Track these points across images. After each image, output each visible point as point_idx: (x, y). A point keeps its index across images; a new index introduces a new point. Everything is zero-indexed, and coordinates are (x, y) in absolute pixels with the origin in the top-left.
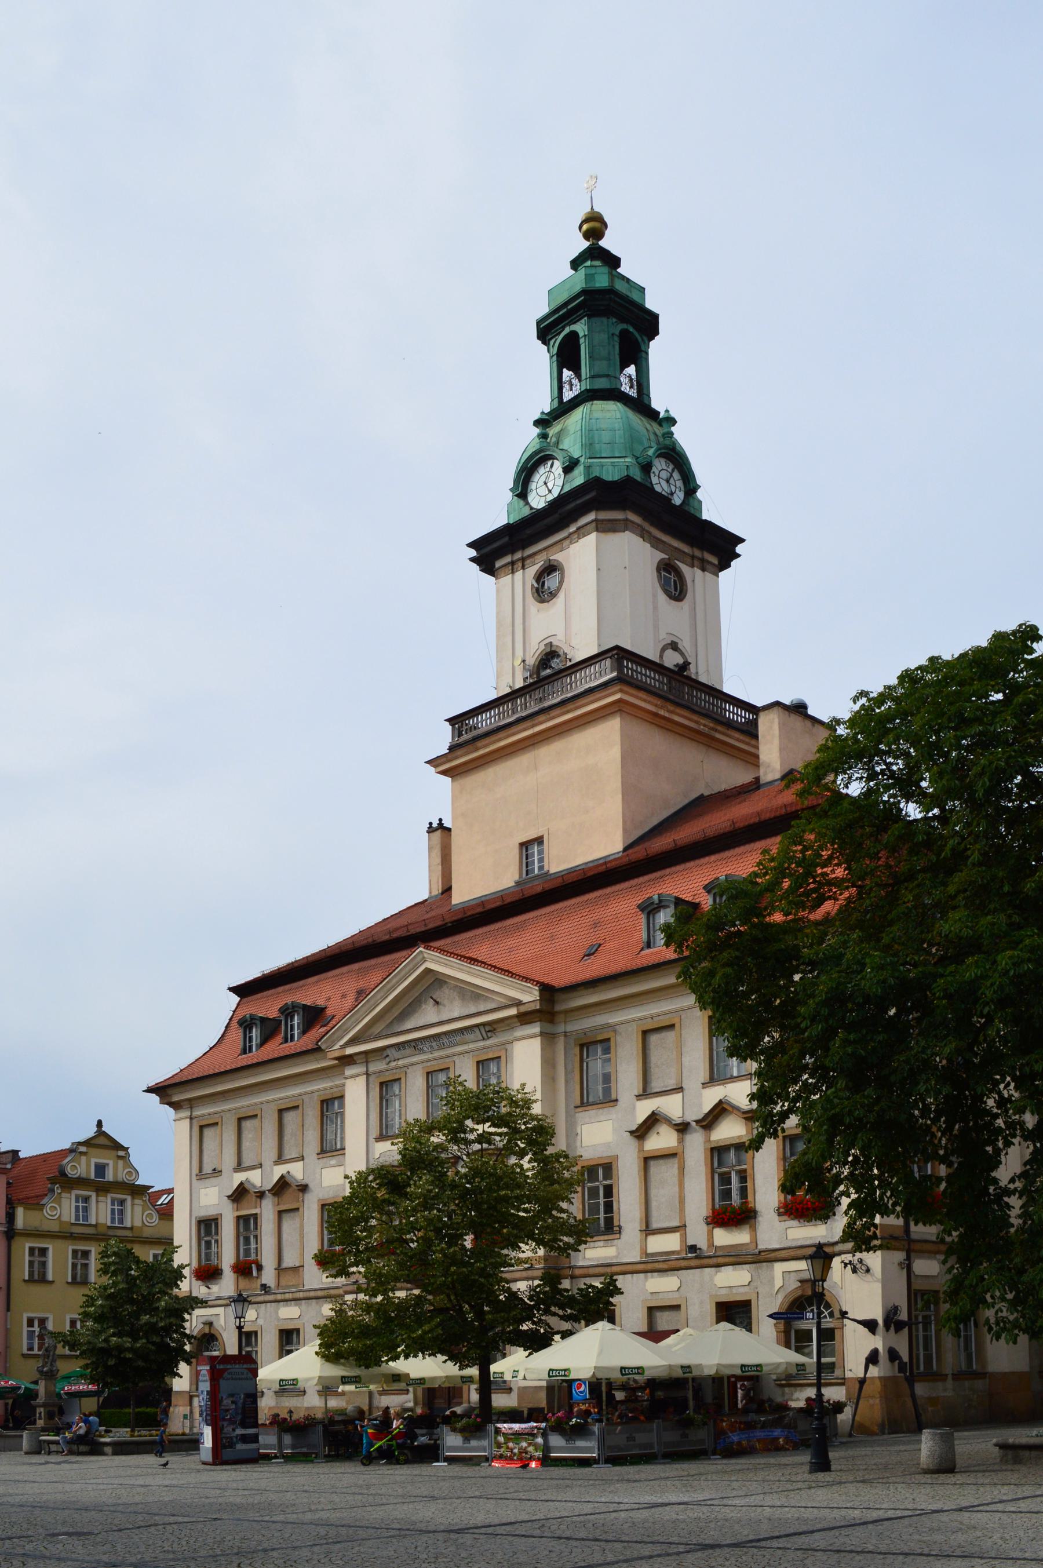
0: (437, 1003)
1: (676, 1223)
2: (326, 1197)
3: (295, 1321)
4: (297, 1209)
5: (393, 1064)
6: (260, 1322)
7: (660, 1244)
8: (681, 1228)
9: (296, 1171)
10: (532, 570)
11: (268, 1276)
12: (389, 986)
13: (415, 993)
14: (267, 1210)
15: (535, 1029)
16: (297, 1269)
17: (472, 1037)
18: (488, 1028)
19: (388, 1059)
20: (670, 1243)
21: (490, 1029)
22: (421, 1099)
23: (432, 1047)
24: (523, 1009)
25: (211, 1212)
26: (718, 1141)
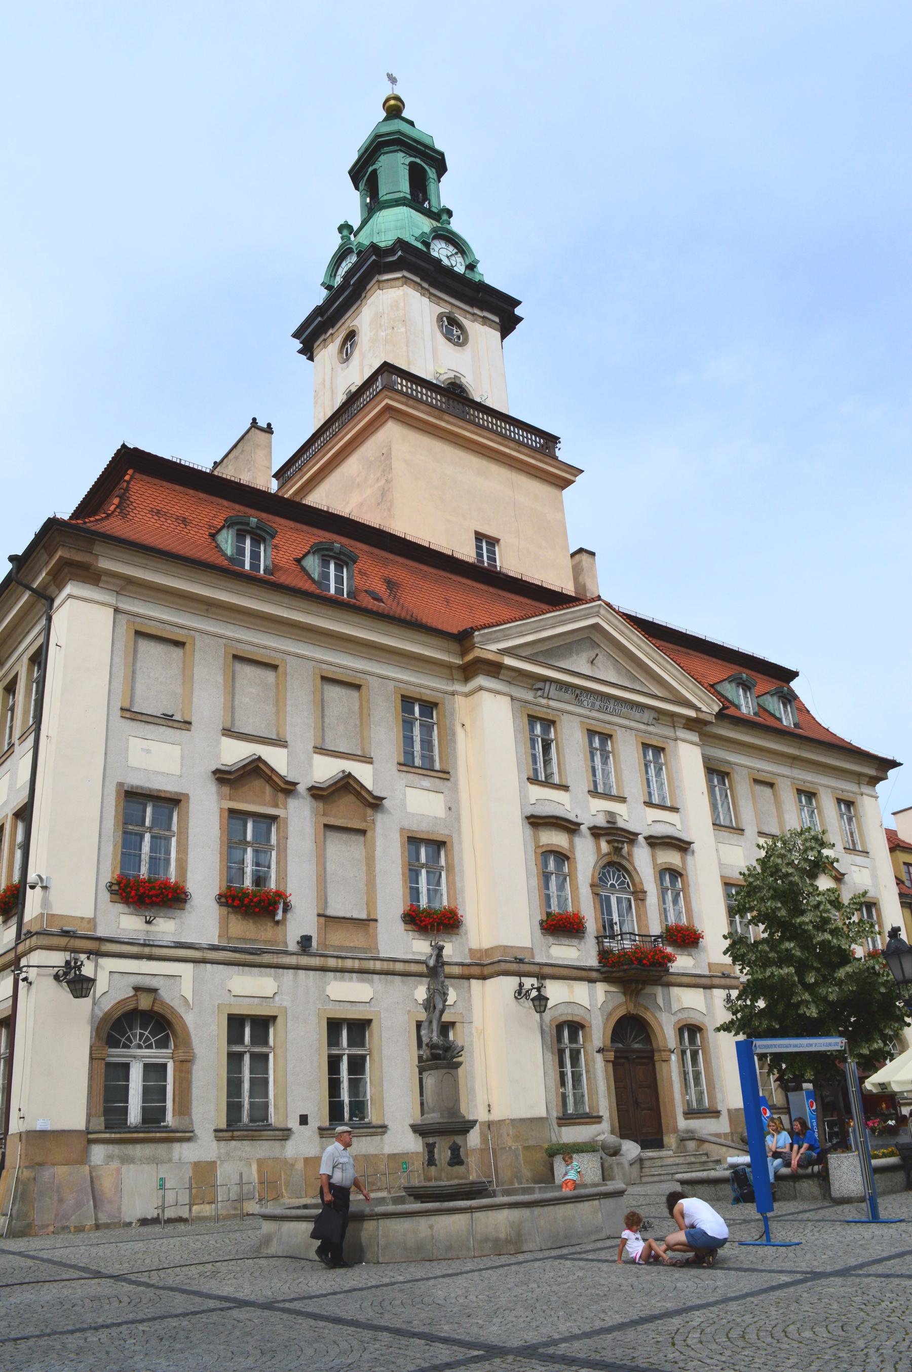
3: (361, 1007)
4: (363, 832)
5: (543, 701)
6: (283, 1001)
11: (301, 921)
12: (563, 618)
14: (299, 816)
16: (366, 924)
17: (638, 715)
19: (540, 693)
22: (582, 755)
23: (593, 704)
24: (701, 716)
25: (168, 786)
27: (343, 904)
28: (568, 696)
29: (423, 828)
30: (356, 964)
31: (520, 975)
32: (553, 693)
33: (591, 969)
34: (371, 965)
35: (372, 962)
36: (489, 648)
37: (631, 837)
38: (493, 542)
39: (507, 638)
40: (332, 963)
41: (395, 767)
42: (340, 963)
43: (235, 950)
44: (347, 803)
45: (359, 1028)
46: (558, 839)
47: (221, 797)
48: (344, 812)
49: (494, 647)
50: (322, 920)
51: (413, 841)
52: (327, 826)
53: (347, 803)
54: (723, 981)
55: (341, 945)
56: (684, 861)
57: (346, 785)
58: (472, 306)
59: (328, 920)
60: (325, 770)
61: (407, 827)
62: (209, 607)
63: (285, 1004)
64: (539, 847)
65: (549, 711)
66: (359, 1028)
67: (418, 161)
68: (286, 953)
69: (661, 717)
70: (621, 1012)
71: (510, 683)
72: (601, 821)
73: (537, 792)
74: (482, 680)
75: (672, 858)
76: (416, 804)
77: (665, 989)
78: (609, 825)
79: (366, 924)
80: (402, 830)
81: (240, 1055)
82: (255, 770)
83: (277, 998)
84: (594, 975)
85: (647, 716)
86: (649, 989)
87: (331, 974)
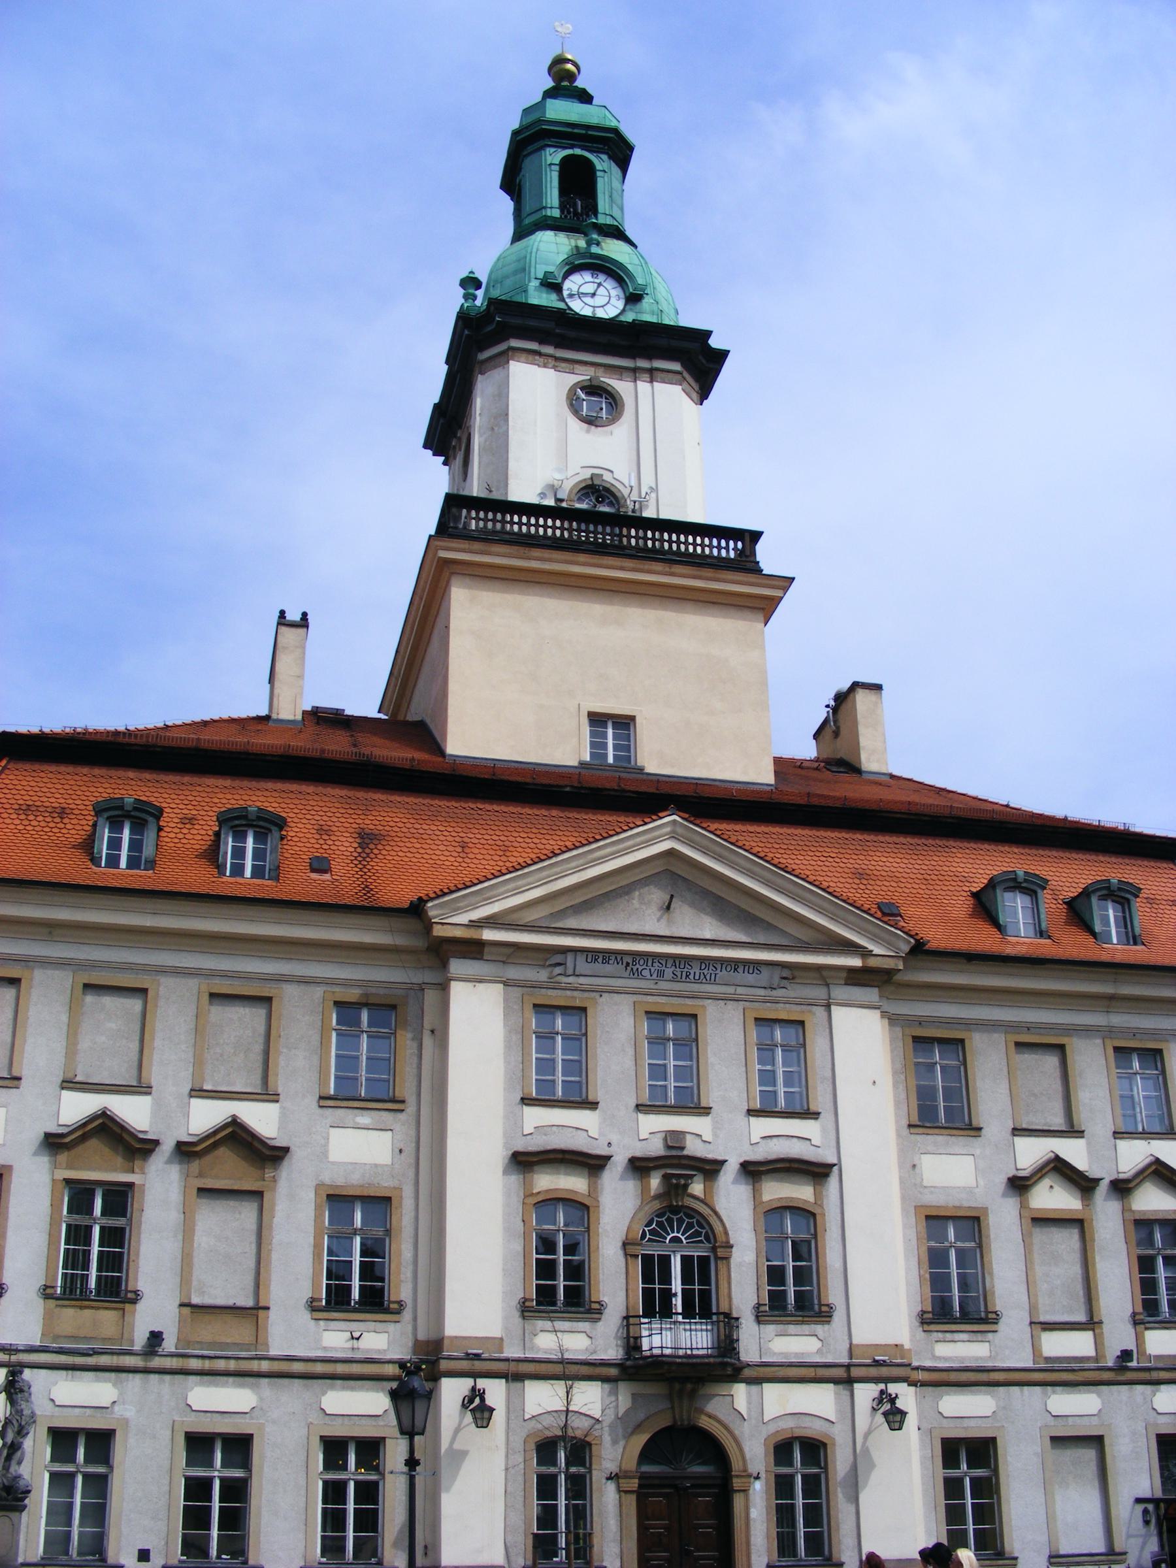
0: (668, 908)
1: (1081, 1317)
2: (340, 1181)
3: (238, 1419)
6: (127, 1411)
7: (1059, 1345)
8: (1092, 1324)
9: (262, 1119)
10: (573, 379)
13: (624, 881)
15: (872, 994)
17: (751, 978)
18: (786, 973)
19: (558, 970)
20: (1079, 1344)
21: (792, 972)
23: (661, 974)
24: (872, 962)
26: (1144, 1212)
27: (224, 1286)
28: (609, 968)
29: (352, 1181)
30: (232, 1365)
31: (475, 1375)
32: (582, 966)
33: (604, 1364)
34: (255, 1366)
35: (256, 1362)
36: (452, 919)
37: (710, 1169)
38: (625, 723)
39: (489, 900)
40: (194, 1364)
41: (312, 1101)
42: (207, 1365)
43: (60, 1351)
44: (241, 1160)
45: (239, 1446)
46: (573, 1183)
47: (55, 1166)
48: (229, 1169)
49: (463, 919)
50: (187, 1310)
51: (338, 1201)
52: (202, 1191)
53: (241, 1160)
54: (873, 1372)
55: (225, 1336)
56: (818, 1196)
57: (236, 1136)
58: (633, 357)
59: (194, 1310)
60: (205, 1116)
61: (327, 1181)
62: (50, 929)
63: (128, 1414)
64: (532, 1195)
65: (576, 994)
66: (239, 1446)
67: (578, 151)
68: (130, 1353)
69: (796, 973)
70: (664, 1422)
71: (504, 962)
72: (656, 1148)
73: (535, 1117)
74: (457, 966)
75: (801, 1192)
76: (361, 1148)
77: (754, 1389)
78: (674, 1153)
79: (255, 1312)
80: (319, 1187)
81: (72, 1476)
82: (105, 1129)
83: (116, 1408)
84: (613, 1372)
85: (765, 976)
86: (722, 1389)
87: (192, 1379)
